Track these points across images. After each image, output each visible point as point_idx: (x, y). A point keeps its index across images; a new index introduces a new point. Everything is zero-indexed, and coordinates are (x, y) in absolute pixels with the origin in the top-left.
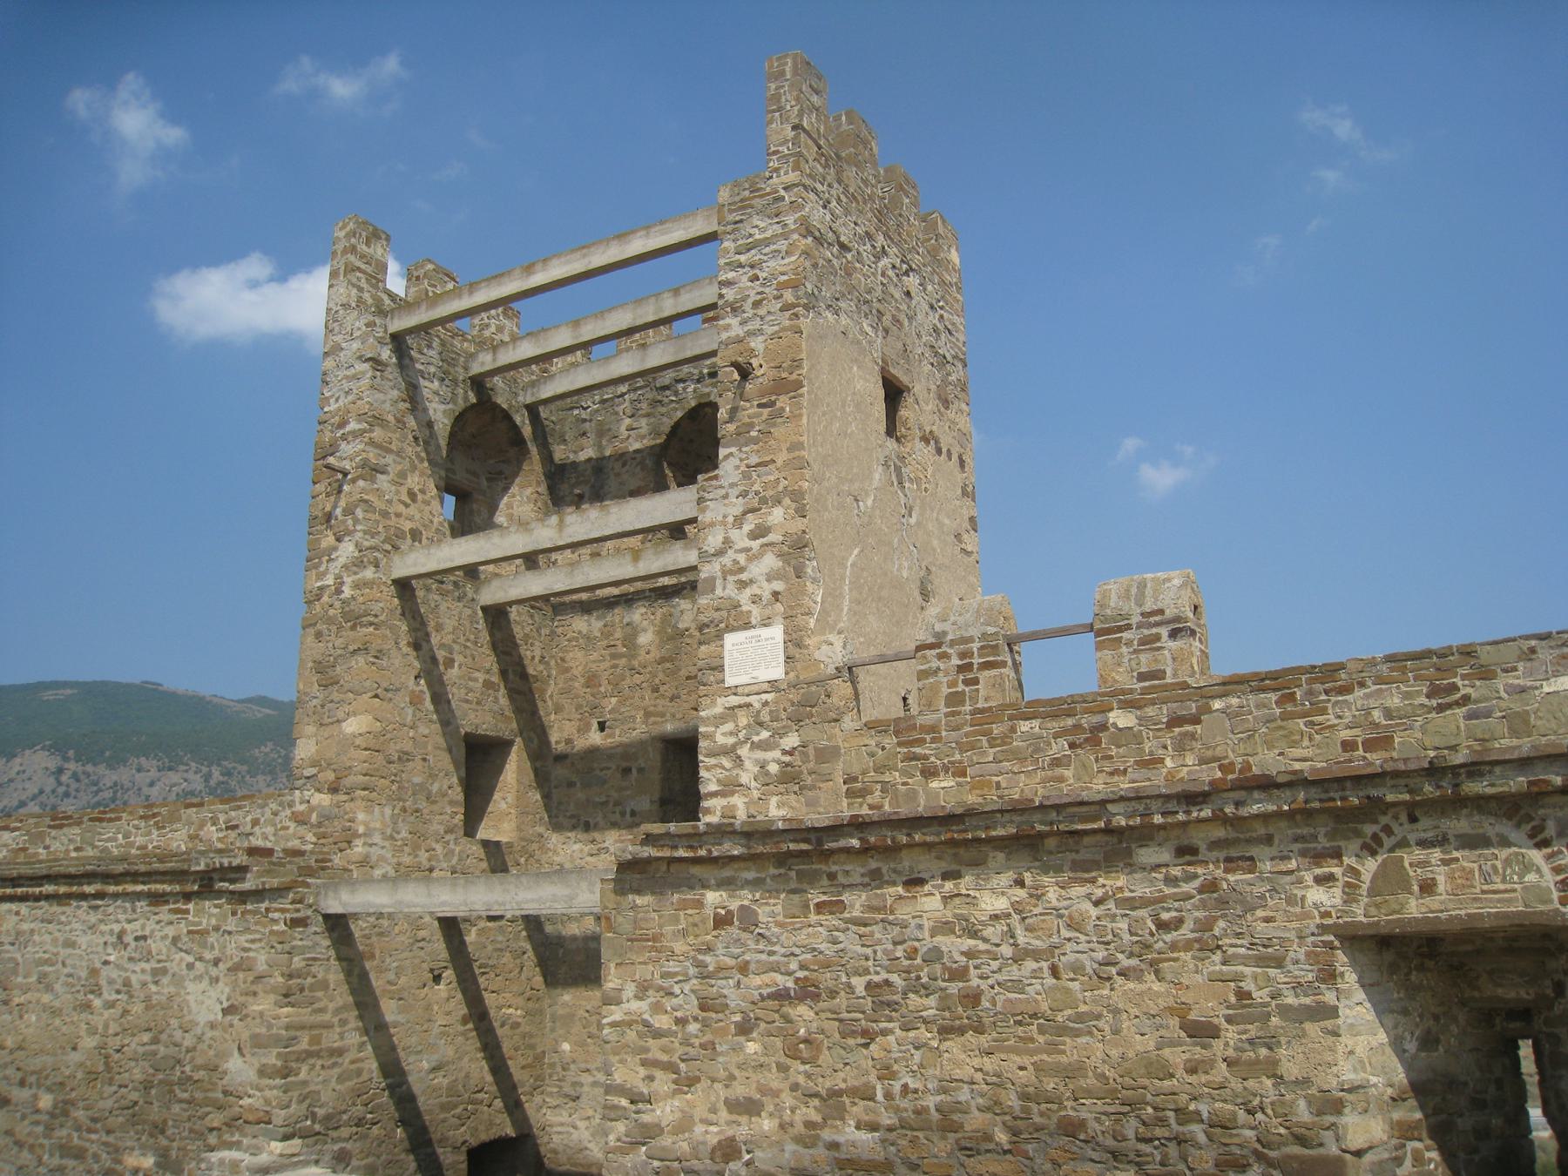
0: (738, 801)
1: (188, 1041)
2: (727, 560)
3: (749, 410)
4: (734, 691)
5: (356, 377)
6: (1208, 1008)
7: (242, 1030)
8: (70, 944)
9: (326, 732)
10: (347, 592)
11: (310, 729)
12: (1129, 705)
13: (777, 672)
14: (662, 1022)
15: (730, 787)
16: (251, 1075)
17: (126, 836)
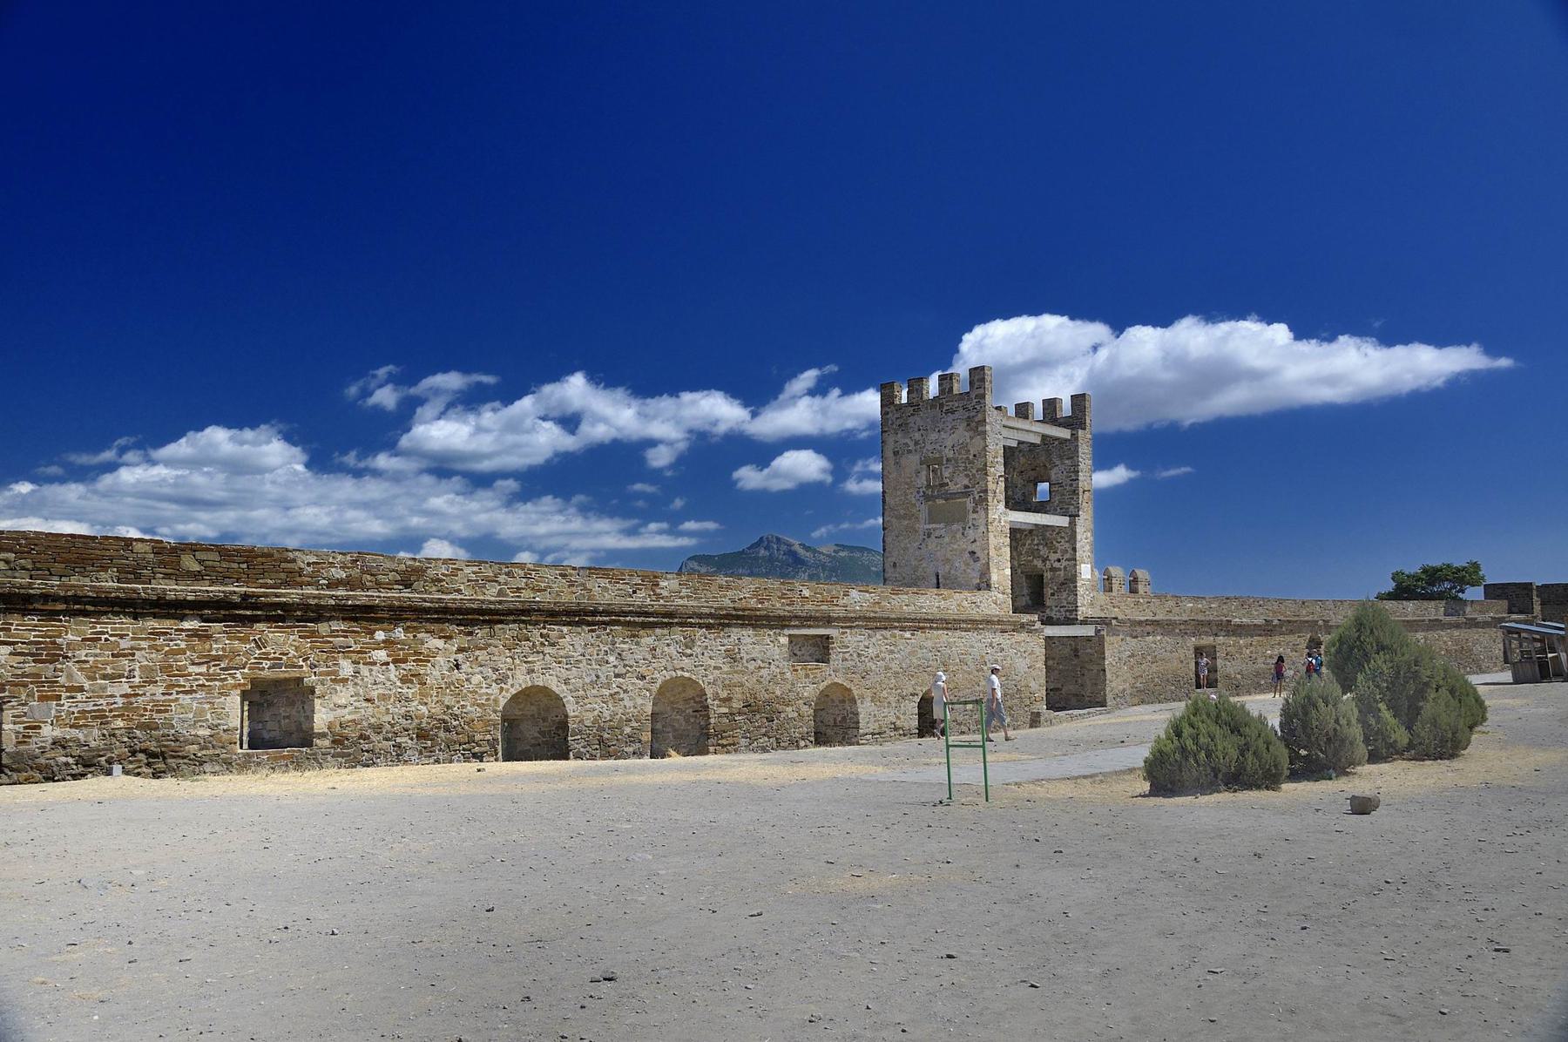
0: (1084, 609)
1: (1019, 678)
2: (1081, 543)
3: (1084, 504)
4: (1083, 580)
5: (998, 439)
6: (1182, 659)
7: (1034, 673)
8: (973, 647)
9: (1001, 572)
10: (1003, 524)
11: (996, 570)
12: (1143, 598)
13: (1090, 577)
14: (1114, 664)
15: (1083, 605)
16: (1037, 686)
17: (930, 602)
